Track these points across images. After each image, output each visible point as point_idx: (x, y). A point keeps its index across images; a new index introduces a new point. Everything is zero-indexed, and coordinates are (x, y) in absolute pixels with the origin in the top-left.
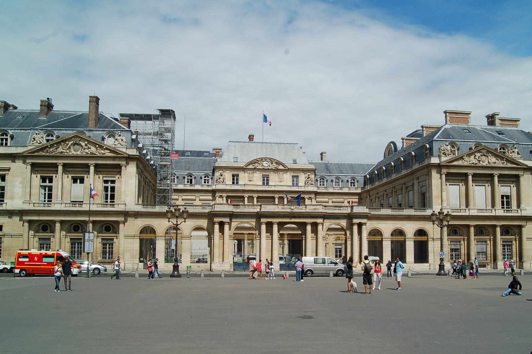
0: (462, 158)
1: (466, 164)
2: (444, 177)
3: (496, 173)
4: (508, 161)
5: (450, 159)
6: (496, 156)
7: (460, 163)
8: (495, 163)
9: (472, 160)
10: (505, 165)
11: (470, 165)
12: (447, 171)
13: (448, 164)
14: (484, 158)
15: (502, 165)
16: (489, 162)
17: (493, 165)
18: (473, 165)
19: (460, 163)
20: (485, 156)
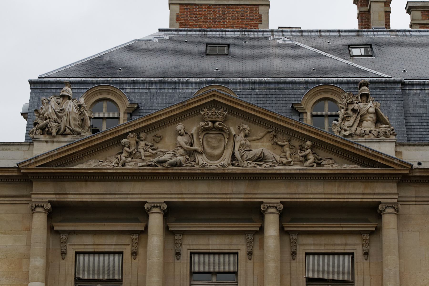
0: (116, 142)
1: (131, 166)
2: (40, 220)
3: (271, 195)
4: (318, 145)
5: (60, 151)
6: (275, 129)
7: (108, 163)
8: (261, 159)
9: (170, 149)
10: (308, 166)
11: (148, 170)
12: (53, 198)
13: (52, 170)
14: (214, 142)
15: (297, 167)
16: (233, 157)
17: (250, 167)
18: (160, 170)
19: (108, 163)
20: (221, 131)
